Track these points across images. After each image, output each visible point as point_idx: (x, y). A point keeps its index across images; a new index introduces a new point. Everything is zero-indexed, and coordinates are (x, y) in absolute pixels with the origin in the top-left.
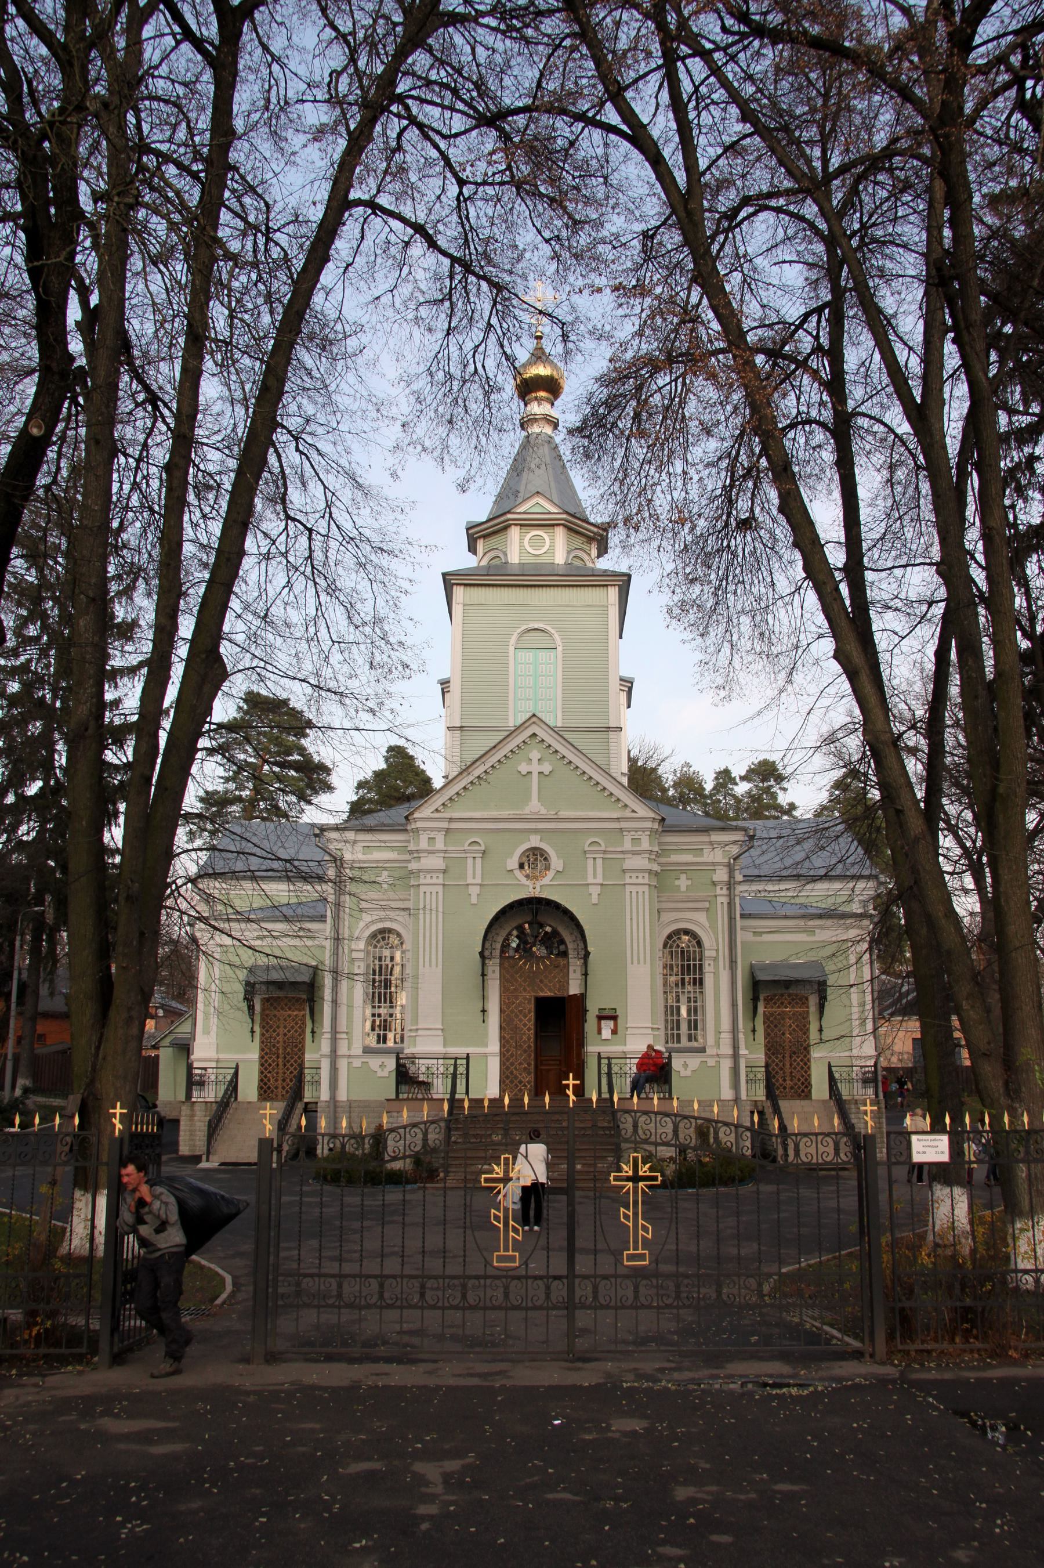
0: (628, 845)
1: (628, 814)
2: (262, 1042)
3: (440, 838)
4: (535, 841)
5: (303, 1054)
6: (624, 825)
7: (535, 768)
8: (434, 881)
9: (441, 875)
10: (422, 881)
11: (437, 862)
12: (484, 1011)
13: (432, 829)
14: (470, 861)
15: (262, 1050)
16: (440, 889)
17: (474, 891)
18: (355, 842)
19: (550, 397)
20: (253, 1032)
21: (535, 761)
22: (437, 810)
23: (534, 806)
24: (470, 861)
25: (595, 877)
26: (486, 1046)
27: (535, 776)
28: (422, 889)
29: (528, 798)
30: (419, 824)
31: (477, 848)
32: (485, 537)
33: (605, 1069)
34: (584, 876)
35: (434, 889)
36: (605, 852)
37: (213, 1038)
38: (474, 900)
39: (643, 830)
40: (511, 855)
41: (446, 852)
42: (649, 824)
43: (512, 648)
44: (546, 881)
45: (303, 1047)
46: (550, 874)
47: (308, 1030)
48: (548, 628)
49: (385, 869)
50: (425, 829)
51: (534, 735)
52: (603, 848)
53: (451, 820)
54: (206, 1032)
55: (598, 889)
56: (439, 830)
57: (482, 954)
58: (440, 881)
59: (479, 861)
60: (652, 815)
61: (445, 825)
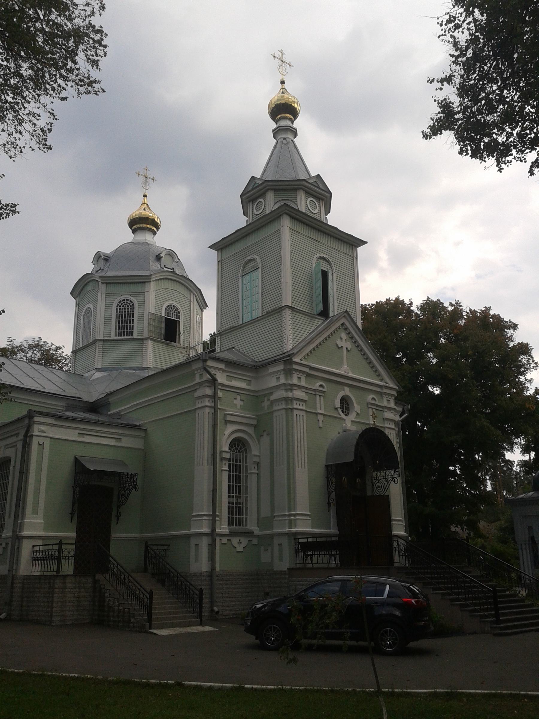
0: (385, 404)
3: (303, 378)
4: (347, 391)
5: (110, 533)
6: (385, 390)
8: (301, 407)
14: (318, 397)
22: (301, 360)
29: (342, 363)
31: (322, 389)
36: (377, 406)
37: (39, 520)
39: (392, 395)
41: (306, 388)
45: (110, 526)
47: (114, 513)
48: (330, 260)
49: (239, 394)
50: (297, 370)
51: (343, 324)
53: (311, 368)
54: (35, 511)
56: (303, 372)
58: (304, 408)
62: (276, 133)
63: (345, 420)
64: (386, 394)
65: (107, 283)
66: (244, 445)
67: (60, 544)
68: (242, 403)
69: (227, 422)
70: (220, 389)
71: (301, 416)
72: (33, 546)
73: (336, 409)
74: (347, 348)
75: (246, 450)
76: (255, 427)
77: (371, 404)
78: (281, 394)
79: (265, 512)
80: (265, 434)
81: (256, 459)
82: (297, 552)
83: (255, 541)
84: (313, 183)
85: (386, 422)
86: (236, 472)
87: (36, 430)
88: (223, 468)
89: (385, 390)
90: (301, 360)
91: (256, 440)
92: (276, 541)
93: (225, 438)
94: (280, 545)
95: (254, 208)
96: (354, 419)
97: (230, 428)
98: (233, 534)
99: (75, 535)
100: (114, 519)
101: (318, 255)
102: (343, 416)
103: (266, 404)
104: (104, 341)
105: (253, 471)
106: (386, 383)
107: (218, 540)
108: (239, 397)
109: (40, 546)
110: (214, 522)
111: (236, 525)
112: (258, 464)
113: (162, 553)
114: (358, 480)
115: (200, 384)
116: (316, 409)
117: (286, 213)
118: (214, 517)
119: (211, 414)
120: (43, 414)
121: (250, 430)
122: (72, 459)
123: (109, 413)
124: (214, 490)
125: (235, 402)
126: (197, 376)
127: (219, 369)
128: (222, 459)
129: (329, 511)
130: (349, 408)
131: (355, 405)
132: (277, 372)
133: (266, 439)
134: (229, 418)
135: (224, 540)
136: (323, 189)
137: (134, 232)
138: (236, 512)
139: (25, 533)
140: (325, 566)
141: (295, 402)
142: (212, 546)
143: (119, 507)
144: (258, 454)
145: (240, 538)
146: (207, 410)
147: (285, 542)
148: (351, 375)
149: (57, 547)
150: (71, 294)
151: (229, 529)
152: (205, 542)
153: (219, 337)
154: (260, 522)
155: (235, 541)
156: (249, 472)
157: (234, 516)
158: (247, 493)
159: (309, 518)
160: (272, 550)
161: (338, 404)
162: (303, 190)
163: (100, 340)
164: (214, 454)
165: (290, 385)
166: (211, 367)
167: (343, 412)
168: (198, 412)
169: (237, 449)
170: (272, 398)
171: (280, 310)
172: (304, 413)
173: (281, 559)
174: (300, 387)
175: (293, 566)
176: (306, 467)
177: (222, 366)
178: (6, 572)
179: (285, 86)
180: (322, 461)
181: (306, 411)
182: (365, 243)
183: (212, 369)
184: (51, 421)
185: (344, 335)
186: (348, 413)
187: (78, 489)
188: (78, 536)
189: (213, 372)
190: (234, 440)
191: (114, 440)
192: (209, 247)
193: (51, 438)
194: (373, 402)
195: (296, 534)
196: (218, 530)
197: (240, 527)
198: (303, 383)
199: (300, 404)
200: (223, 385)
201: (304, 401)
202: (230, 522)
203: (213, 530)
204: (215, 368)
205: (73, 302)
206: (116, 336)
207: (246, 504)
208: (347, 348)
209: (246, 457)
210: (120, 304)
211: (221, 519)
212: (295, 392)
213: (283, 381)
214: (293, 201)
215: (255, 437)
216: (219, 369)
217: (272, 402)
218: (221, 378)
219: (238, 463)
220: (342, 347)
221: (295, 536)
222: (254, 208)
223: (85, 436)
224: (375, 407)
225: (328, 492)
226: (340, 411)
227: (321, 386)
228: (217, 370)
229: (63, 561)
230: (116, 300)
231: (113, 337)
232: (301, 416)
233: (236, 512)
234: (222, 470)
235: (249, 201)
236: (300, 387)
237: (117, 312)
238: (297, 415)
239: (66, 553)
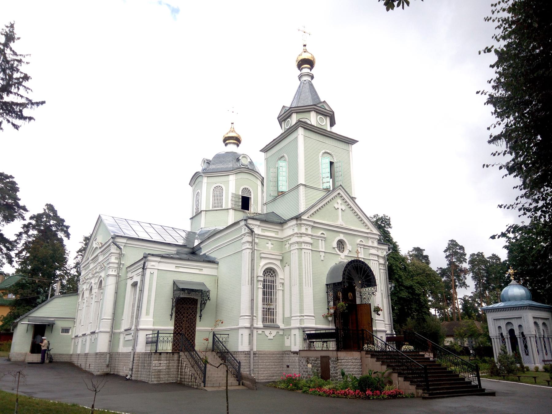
0: (370, 244)
2: (176, 321)
3: (310, 229)
4: (341, 237)
5: (195, 327)
6: (370, 235)
7: (340, 207)
8: (308, 248)
11: (308, 239)
13: (307, 225)
14: (320, 241)
15: (175, 324)
18: (259, 226)
19: (311, 67)
20: (171, 315)
21: (339, 204)
22: (308, 217)
23: (340, 222)
26: (290, 325)
29: (337, 219)
30: (303, 222)
32: (297, 113)
35: (308, 251)
36: (364, 245)
37: (150, 319)
38: (322, 258)
39: (375, 239)
41: (312, 236)
43: (320, 158)
45: (195, 323)
49: (270, 240)
50: (304, 224)
51: (339, 194)
53: (315, 222)
54: (147, 314)
56: (309, 225)
58: (310, 248)
60: (379, 234)
61: (312, 224)
62: (300, 77)
63: (340, 255)
64: (371, 238)
65: (207, 177)
66: (274, 272)
67: (158, 333)
68: (272, 246)
69: (261, 258)
70: (257, 238)
71: (308, 253)
72: (146, 335)
73: (334, 248)
74: (342, 209)
75: (275, 275)
76: (281, 261)
77: (360, 244)
78: (295, 239)
79: (287, 315)
80: (287, 265)
81: (282, 281)
82: (305, 340)
83: (281, 333)
84: (321, 107)
85: (371, 256)
86: (269, 289)
87: (149, 265)
88: (259, 287)
89: (370, 235)
90: (308, 217)
91: (282, 269)
92: (293, 332)
93: (260, 268)
94: (295, 335)
95: (285, 125)
96: (347, 255)
97: (264, 262)
98: (265, 327)
99: (173, 328)
100: (198, 318)
101: (324, 151)
102: (339, 252)
103: (288, 246)
104: (206, 211)
105: (280, 289)
107: (255, 331)
108: (270, 242)
109: (149, 334)
110: (252, 320)
111: (271, 322)
112: (283, 284)
113: (224, 339)
115: (244, 235)
116: (319, 248)
117: (301, 126)
118: (252, 317)
119: (250, 253)
120: (153, 255)
121: (278, 263)
122: (172, 283)
123: (201, 254)
124: (252, 300)
125: (267, 245)
126: (243, 230)
127: (256, 225)
128: (258, 281)
130: (344, 248)
131: (348, 245)
132: (293, 226)
133: (287, 268)
134: (263, 255)
135: (260, 332)
136: (328, 110)
137: (226, 145)
138: (269, 314)
139: (141, 327)
140: (320, 349)
142: (251, 335)
143: (201, 311)
144: (283, 278)
145: (271, 330)
146: (248, 251)
147: (297, 332)
148: (345, 226)
149: (156, 335)
150: (190, 184)
151: (263, 324)
152: (246, 333)
153: (266, 206)
154: (284, 320)
155: (267, 332)
156: (277, 289)
158: (276, 302)
159: (313, 318)
160: (291, 338)
161: (335, 245)
162: (315, 111)
163: (203, 211)
164: (252, 278)
165: (301, 234)
166: (250, 224)
167: (339, 250)
168: (244, 252)
169: (269, 275)
170: (290, 242)
171: (298, 186)
172: (310, 251)
173: (295, 345)
174: (307, 235)
175: (301, 349)
176: (312, 285)
177: (258, 223)
178: (131, 351)
179: (307, 47)
180: (324, 281)
181: (312, 250)
182: (357, 141)
183: (251, 225)
184: (158, 259)
185: (339, 201)
186: (343, 251)
187: (174, 300)
188: (175, 328)
189: (251, 227)
190: (267, 269)
191: (198, 270)
192: (260, 151)
193: (158, 269)
194: (361, 243)
195: (303, 328)
196: (255, 325)
197: (271, 324)
198: (309, 232)
200: (259, 235)
201: (311, 244)
202: (264, 320)
203: (252, 325)
204: (253, 225)
205: (190, 189)
206: (212, 208)
207: (276, 309)
208: (342, 209)
209: (276, 279)
210: (215, 189)
211: (257, 318)
212: (303, 238)
213: (296, 231)
214: (308, 119)
215: (281, 268)
216: (256, 225)
217: (291, 244)
218: (257, 231)
219: (270, 284)
220: (338, 208)
221: (303, 329)
222: (285, 125)
223: (180, 268)
224: (363, 247)
225: (328, 301)
227: (322, 234)
228: (254, 226)
229: (160, 344)
230: (213, 187)
231: (211, 209)
232: (308, 253)
233: (269, 314)
234: (258, 288)
235: (283, 121)
236: (307, 235)
237: (213, 193)
239: (161, 339)
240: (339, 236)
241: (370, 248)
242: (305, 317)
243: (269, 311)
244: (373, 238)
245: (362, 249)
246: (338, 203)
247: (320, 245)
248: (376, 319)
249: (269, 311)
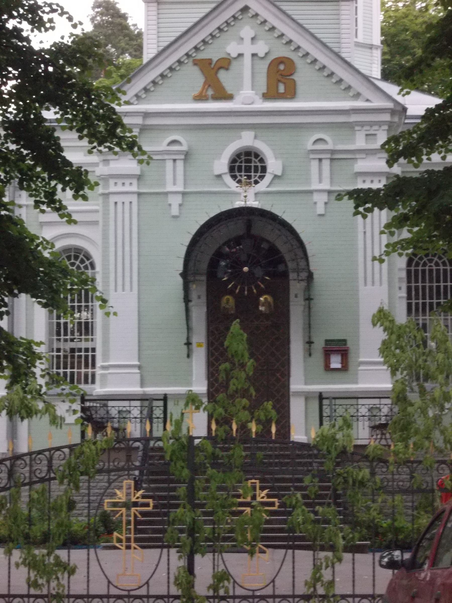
1: (359, 104)
6: (353, 118)
8: (127, 188)
9: (135, 182)
10: (113, 189)
12: (188, 344)
14: (169, 164)
16: (134, 199)
17: (175, 201)
21: (248, 41)
24: (169, 164)
25: (320, 181)
27: (247, 60)
28: (113, 199)
33: (327, 411)
34: (308, 181)
35: (127, 199)
36: (333, 152)
38: (175, 211)
39: (380, 124)
40: (219, 155)
42: (387, 117)
44: (262, 186)
46: (268, 178)
51: (245, 9)
52: (330, 147)
55: (324, 197)
57: (184, 275)
58: (134, 188)
59: (180, 165)
64: (362, 124)
73: (219, 176)
74: (254, 55)
85: (360, 180)
89: (353, 118)
106: (368, 100)
114: (228, 300)
129: (188, 356)
141: (112, 182)
157: (83, 370)
199: (123, 184)
220: (240, 55)
226: (228, 179)
227: (174, 142)
238: (116, 203)
240: (240, 137)
241: (357, 156)
242: (111, 371)
243: (73, 357)
244: (371, 124)
245: (326, 164)
246: (242, 39)
247: (169, 177)
248: (361, 359)
249: (73, 357)
